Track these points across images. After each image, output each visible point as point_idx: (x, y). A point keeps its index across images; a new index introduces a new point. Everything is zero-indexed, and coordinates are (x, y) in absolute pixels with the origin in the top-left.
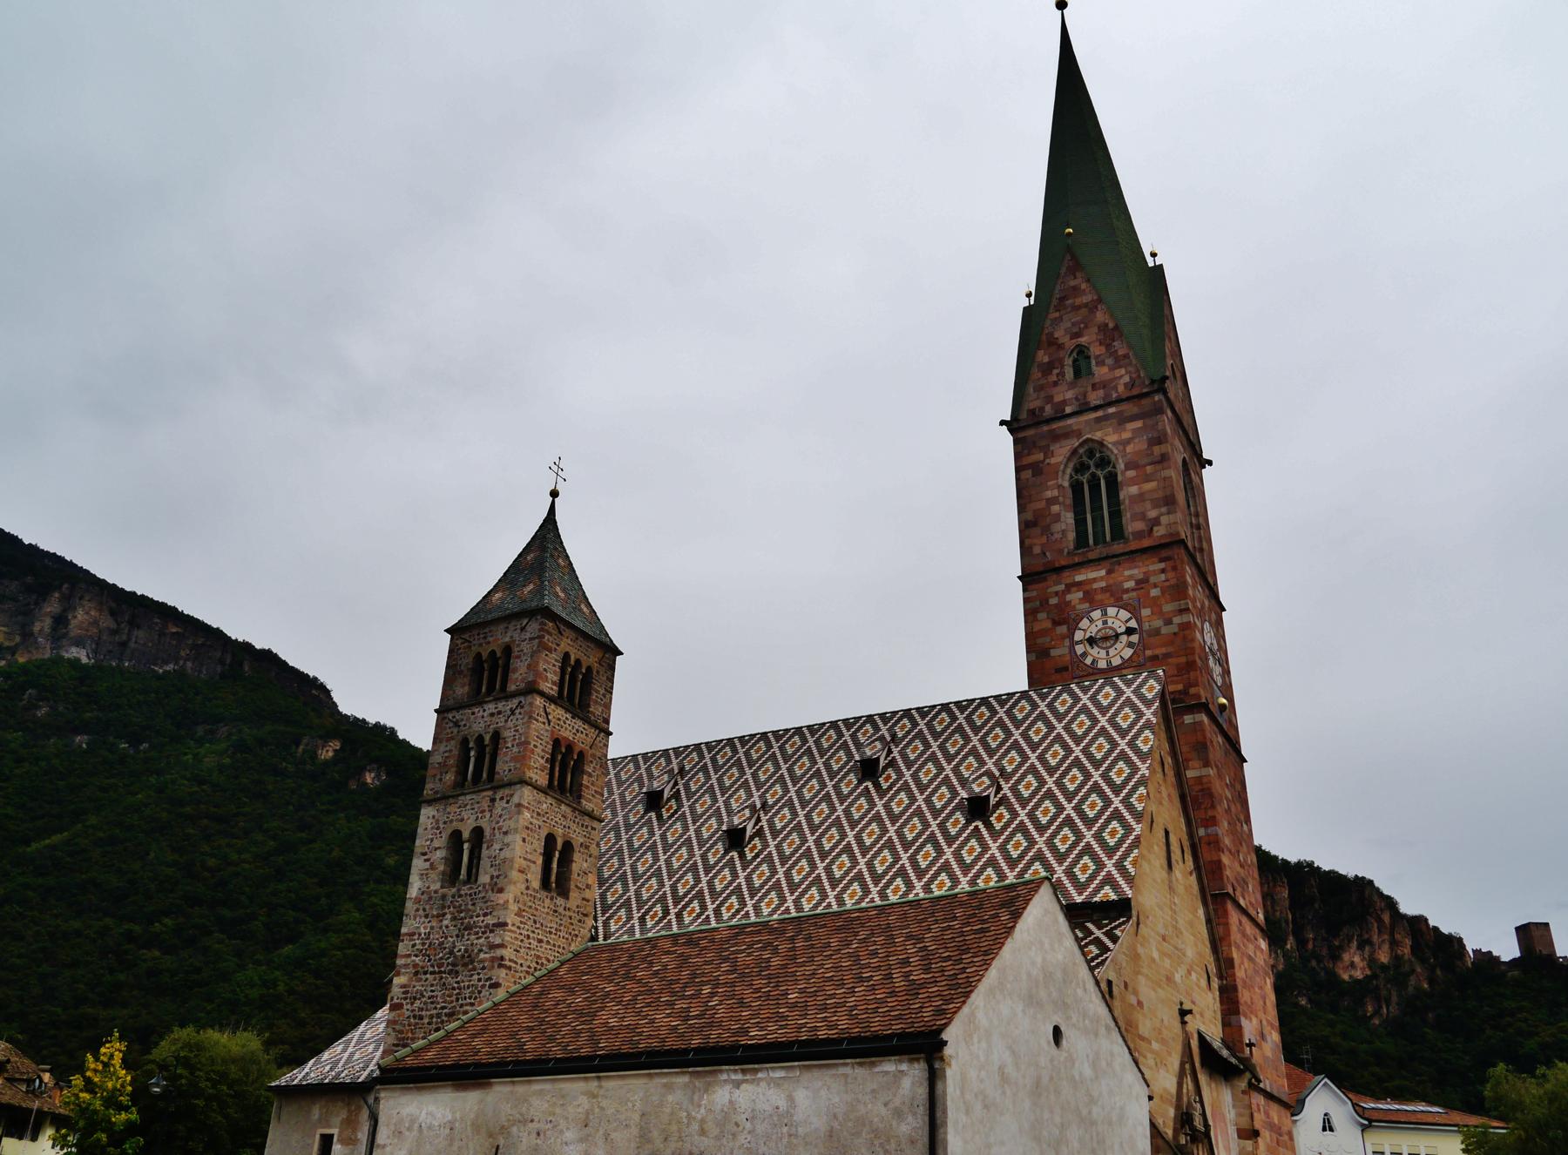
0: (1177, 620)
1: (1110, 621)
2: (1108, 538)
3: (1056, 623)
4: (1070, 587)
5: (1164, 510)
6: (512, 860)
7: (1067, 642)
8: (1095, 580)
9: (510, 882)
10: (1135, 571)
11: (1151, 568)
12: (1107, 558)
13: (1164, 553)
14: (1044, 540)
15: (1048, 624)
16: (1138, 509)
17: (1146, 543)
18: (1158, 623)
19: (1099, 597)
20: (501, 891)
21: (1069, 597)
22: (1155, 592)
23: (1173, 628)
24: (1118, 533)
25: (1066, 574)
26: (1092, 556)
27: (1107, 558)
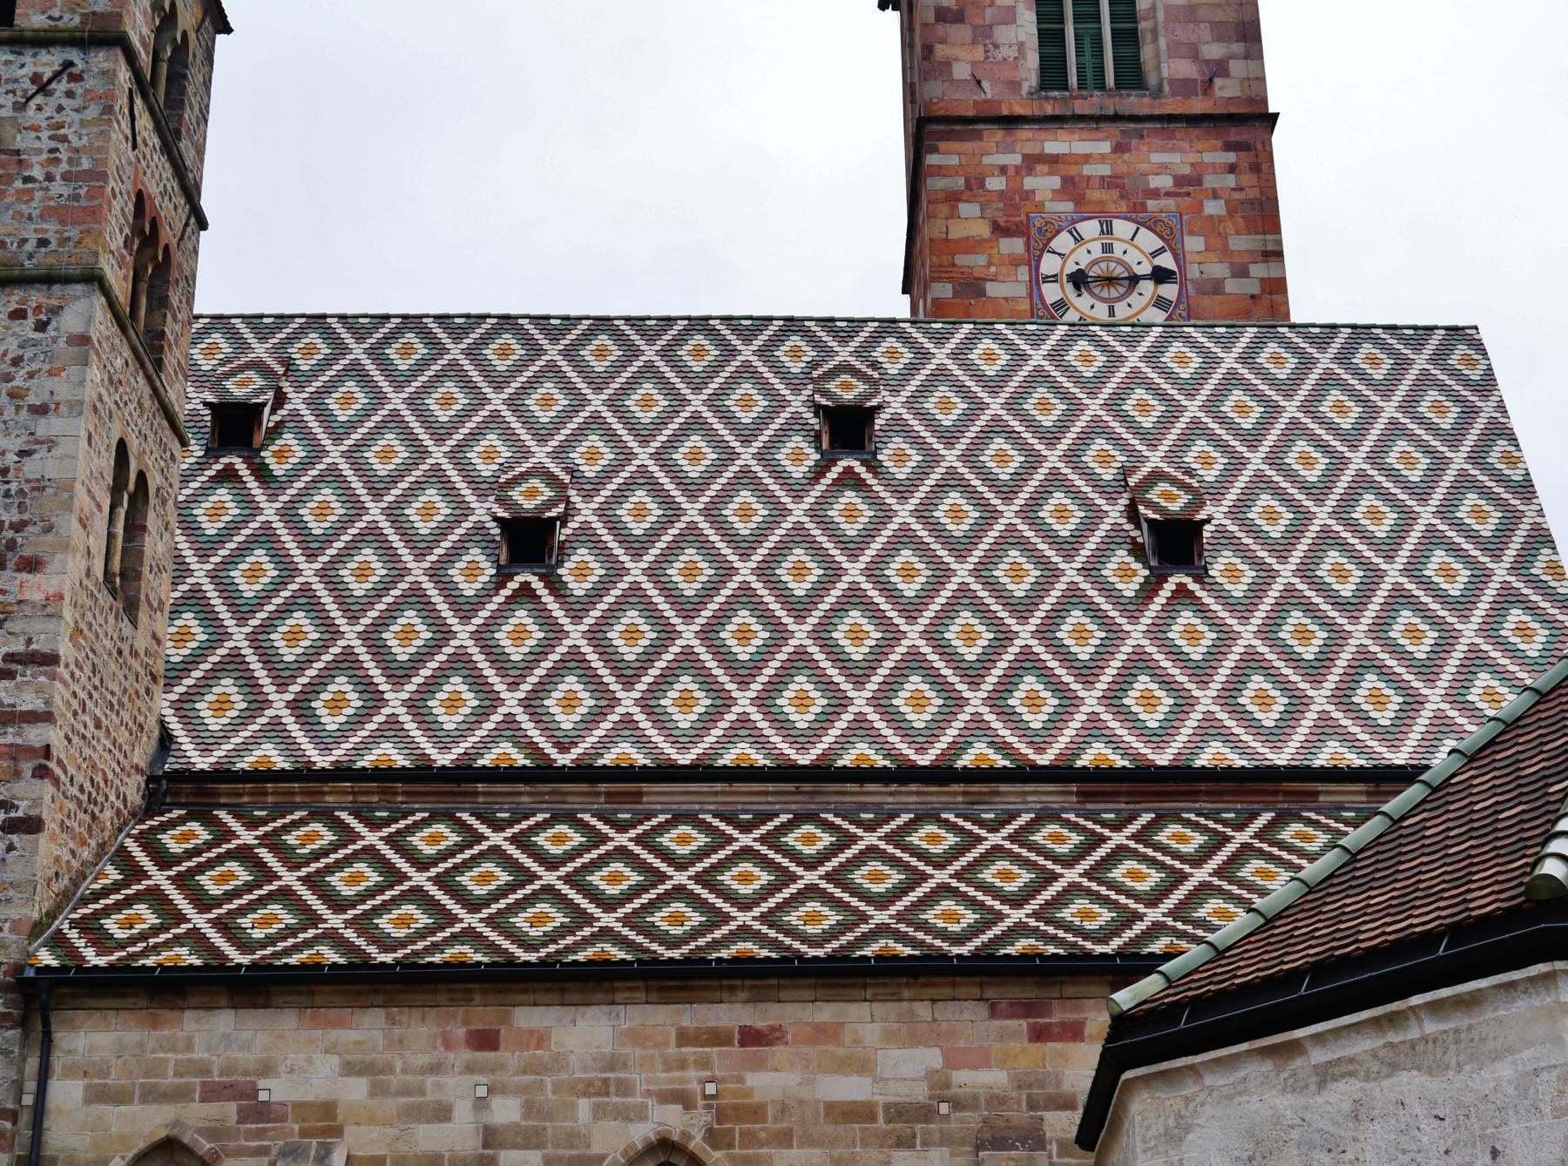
0: (1258, 270)
1: (1118, 248)
2: (1110, 80)
3: (1000, 230)
4: (1032, 162)
5: (1238, 48)
6: (68, 486)
7: (1023, 273)
8: (1087, 158)
9: (65, 547)
10: (1175, 158)
11: (1208, 158)
12: (1117, 118)
13: (1235, 135)
14: (978, 53)
15: (984, 230)
16: (1183, 34)
17: (1198, 106)
18: (1218, 270)
19: (1095, 194)
20: (32, 565)
21: (1029, 183)
22: (1213, 208)
23: (1250, 286)
24: (1132, 75)
25: (1024, 133)
26: (1080, 107)
27: (1117, 118)
